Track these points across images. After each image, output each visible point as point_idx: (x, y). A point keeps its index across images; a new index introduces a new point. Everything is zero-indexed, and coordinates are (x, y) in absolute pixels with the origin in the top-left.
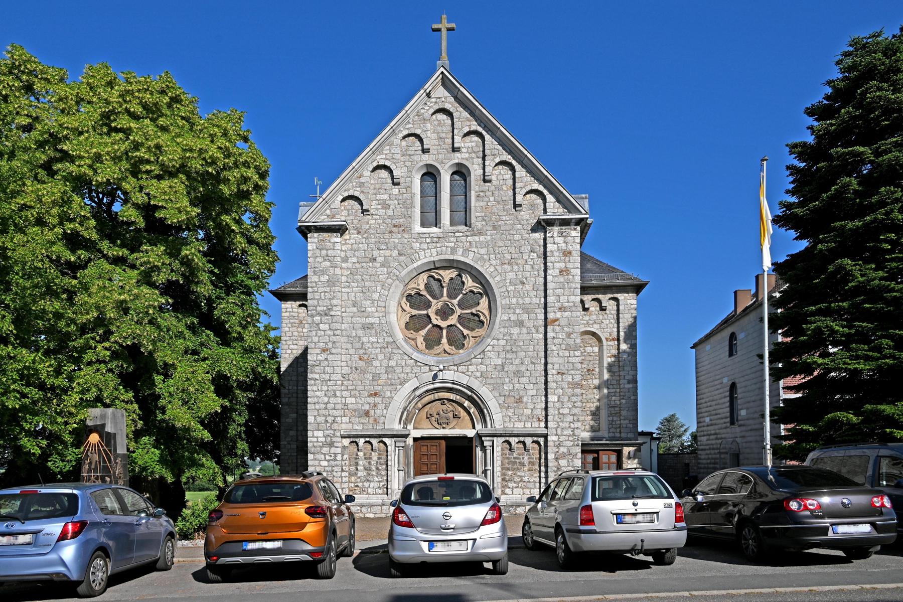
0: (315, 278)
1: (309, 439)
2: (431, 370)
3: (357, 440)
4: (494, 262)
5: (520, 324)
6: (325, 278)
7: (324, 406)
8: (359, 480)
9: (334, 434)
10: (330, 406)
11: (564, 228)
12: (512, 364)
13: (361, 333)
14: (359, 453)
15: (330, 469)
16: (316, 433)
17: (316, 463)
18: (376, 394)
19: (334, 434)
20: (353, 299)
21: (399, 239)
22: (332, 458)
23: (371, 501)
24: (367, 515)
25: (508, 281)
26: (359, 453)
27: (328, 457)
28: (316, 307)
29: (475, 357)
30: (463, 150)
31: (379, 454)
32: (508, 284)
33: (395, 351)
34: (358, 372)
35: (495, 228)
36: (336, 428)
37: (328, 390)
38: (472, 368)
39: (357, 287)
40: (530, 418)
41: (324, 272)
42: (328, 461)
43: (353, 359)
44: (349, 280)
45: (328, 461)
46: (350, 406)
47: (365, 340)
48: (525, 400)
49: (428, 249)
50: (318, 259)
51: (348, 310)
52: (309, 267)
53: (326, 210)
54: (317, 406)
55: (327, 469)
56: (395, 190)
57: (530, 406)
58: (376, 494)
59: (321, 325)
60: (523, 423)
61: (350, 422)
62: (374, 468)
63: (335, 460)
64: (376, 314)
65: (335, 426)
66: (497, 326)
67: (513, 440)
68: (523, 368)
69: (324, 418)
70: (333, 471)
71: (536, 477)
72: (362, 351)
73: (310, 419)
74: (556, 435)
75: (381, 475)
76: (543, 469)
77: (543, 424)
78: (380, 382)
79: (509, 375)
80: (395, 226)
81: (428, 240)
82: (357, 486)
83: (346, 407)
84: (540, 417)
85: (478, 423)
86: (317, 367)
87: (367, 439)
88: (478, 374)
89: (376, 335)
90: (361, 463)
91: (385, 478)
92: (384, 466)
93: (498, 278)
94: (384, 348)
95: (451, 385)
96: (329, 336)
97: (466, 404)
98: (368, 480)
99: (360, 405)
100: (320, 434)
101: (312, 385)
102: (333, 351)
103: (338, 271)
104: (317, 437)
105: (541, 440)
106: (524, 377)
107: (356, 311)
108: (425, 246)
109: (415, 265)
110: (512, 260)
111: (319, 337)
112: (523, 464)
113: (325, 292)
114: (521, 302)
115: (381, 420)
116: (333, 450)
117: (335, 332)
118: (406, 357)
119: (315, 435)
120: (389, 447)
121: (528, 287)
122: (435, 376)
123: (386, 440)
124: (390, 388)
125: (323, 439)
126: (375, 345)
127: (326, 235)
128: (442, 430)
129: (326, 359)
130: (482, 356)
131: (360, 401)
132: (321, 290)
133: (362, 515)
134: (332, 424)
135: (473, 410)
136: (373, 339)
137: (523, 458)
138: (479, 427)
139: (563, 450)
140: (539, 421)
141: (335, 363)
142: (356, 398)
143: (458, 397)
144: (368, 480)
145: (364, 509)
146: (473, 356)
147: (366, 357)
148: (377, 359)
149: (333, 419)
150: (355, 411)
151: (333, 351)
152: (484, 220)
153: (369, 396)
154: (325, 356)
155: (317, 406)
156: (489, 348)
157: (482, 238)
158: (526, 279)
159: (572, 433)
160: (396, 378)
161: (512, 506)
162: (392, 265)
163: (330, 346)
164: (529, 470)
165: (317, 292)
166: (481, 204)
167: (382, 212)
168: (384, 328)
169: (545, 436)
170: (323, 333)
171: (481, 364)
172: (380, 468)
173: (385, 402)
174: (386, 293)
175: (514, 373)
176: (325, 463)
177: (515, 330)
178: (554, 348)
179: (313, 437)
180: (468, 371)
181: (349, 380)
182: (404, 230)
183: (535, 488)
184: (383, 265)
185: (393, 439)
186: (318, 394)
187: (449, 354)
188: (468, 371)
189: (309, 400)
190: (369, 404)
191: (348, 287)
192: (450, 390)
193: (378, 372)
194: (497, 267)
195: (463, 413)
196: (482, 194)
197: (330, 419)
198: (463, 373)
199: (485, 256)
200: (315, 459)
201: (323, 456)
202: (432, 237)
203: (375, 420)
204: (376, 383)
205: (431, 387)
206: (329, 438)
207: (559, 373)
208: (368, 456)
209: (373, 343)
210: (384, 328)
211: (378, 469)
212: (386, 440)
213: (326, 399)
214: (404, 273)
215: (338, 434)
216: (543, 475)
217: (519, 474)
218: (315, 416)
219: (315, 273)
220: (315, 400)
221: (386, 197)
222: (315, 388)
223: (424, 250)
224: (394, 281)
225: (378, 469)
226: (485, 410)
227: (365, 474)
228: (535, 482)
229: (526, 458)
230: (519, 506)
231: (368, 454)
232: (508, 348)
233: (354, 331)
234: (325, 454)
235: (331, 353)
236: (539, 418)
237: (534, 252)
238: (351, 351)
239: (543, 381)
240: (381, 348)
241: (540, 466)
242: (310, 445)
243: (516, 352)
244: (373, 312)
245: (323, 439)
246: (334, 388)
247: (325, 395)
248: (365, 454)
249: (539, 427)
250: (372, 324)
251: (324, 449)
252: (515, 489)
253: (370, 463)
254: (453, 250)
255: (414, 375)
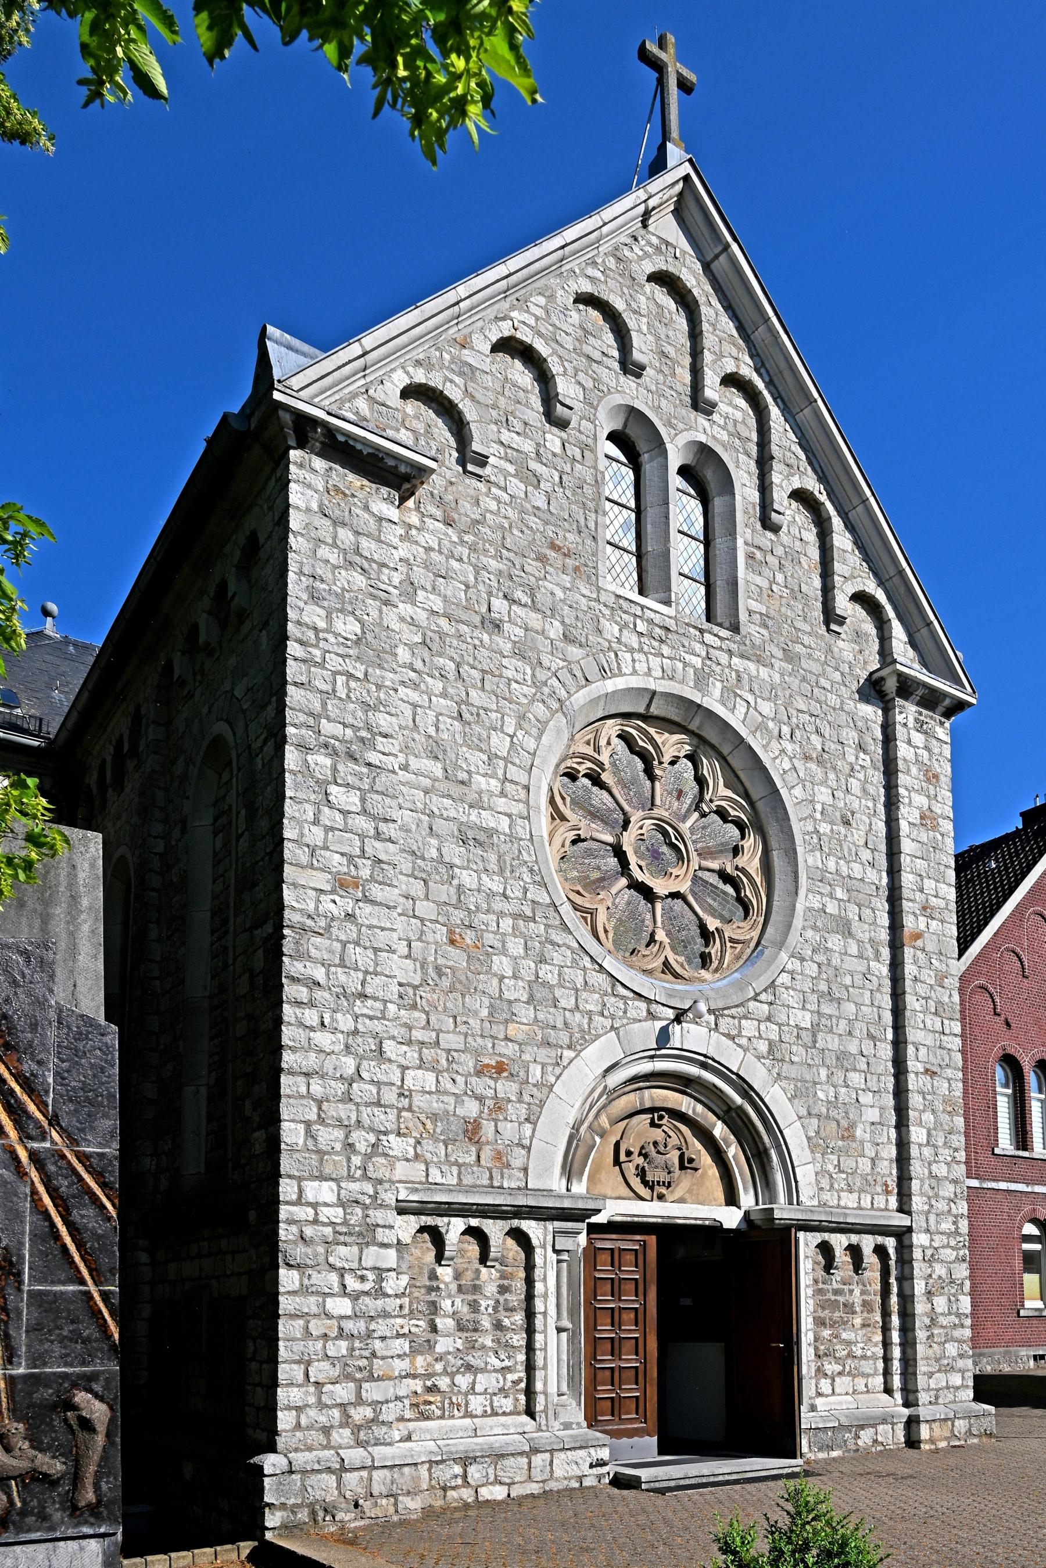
0: (314, 615)
1: (284, 1211)
2: (651, 1016)
3: (440, 1222)
4: (789, 747)
5: (846, 930)
6: (348, 627)
7: (340, 1088)
8: (439, 1367)
9: (374, 1197)
10: (362, 1091)
11: (924, 712)
12: (831, 1031)
13: (454, 852)
14: (440, 1270)
15: (361, 1325)
16: (313, 1190)
17: (311, 1304)
18: (500, 1068)
19: (374, 1197)
20: (432, 731)
21: (565, 589)
22: (367, 1286)
23: (498, 1441)
24: (485, 1493)
25: (819, 807)
26: (440, 1270)
27: (352, 1283)
28: (316, 717)
29: (755, 998)
30: (715, 417)
31: (503, 1276)
32: (818, 816)
33: (558, 937)
34: (445, 983)
35: (789, 657)
36: (383, 1173)
37: (356, 1032)
38: (749, 1027)
39: (444, 695)
40: (868, 1184)
41: (346, 605)
42: (355, 1297)
43: (430, 937)
44: (419, 665)
45: (355, 1297)
46: (418, 1101)
47: (468, 878)
48: (859, 1132)
49: (641, 650)
50: (324, 552)
51: (414, 763)
52: (293, 567)
53: (354, 395)
54: (317, 1088)
55: (349, 1326)
56: (553, 440)
57: (870, 1152)
58: (495, 1414)
59: (333, 789)
60: (856, 1195)
61: (417, 1156)
62: (486, 1323)
63: (379, 1293)
64: (501, 804)
65: (379, 1167)
66: (798, 922)
67: (839, 1242)
68: (853, 1049)
69: (339, 1134)
70: (369, 1334)
71: (876, 1345)
72: (458, 916)
73: (291, 1133)
74: (927, 1231)
75: (507, 1345)
76: (895, 1320)
77: (893, 1202)
78: (512, 1030)
79: (828, 1062)
80: (553, 546)
81: (641, 627)
82: (432, 1389)
83: (405, 1102)
84: (889, 1183)
85: (745, 1189)
86: (318, 940)
87: (474, 1222)
88: (763, 1047)
89: (502, 871)
90: (446, 1304)
91: (521, 1357)
92: (519, 1318)
93: (798, 791)
94: (527, 919)
95: (694, 1070)
96: (362, 837)
97: (719, 1130)
98: (469, 1367)
99: (451, 1100)
100: (323, 1192)
101: (299, 1003)
102: (377, 892)
103: (391, 618)
104: (315, 1206)
105: (890, 1243)
106: (855, 1070)
107: (439, 773)
108: (633, 641)
109: (611, 685)
110: (825, 756)
111: (329, 829)
112: (849, 1308)
113: (350, 676)
114: (844, 870)
115: (517, 1158)
116: (372, 1256)
117: (383, 827)
118: (587, 962)
119: (310, 1195)
120: (538, 1251)
121: (858, 836)
122: (663, 1037)
123: (530, 1227)
124: (543, 1054)
125: (336, 1214)
126: (498, 905)
127: (354, 480)
128: (656, 1204)
129: (350, 916)
130: (771, 998)
131: (449, 1086)
132: (334, 662)
133: (467, 1495)
134: (368, 1157)
135: (733, 1151)
136: (495, 885)
137: (851, 1291)
138: (747, 1200)
139: (940, 1270)
140: (888, 1192)
141: (382, 939)
142: (438, 1073)
143: (700, 1108)
144: (469, 1367)
145: (475, 1473)
146: (752, 994)
147: (469, 937)
148: (504, 952)
149: (372, 1138)
150: (434, 1117)
151: (377, 892)
152: (766, 627)
153: (479, 1073)
154: (349, 905)
155: (317, 1088)
156: (785, 978)
157: (764, 673)
158: (853, 813)
159: (953, 1228)
160: (560, 1024)
161: (848, 1428)
162: (546, 662)
163: (365, 873)
164: (864, 1326)
165: (322, 665)
166: (758, 580)
167: (517, 487)
168: (525, 856)
169: (903, 1235)
170: (339, 817)
171: (769, 1019)
172: (506, 1322)
173: (526, 1098)
174: (531, 744)
175: (838, 1058)
176: (341, 1306)
177: (835, 942)
178: (917, 1006)
179: (299, 1202)
180: (739, 1035)
181: (414, 1007)
182: (576, 569)
183: (875, 1374)
184: (519, 653)
185: (550, 1226)
186: (322, 1039)
187: (677, 976)
188: (739, 1035)
189: (288, 1059)
190: (481, 1099)
191: (416, 686)
192: (683, 1083)
193: (507, 995)
194: (796, 762)
195: (705, 1159)
196: (759, 555)
197: (362, 1140)
198: (728, 1036)
199: (771, 724)
200: (304, 1291)
201: (334, 1278)
202: (651, 622)
203: (498, 1156)
204: (499, 1031)
205: (646, 1067)
206: (358, 1211)
207: (927, 1071)
208: (467, 1279)
209: (491, 895)
210: (525, 856)
211: (498, 1326)
212: (530, 1227)
213: (349, 1065)
214: (580, 697)
215: (390, 1198)
216: (895, 1337)
217: (844, 1336)
218: (308, 1124)
219: (314, 597)
220: (311, 1061)
221: (528, 447)
222: (311, 1017)
223: (632, 650)
224: (553, 713)
225: (498, 1326)
226: (773, 1153)
227: (459, 1344)
228: (874, 1358)
229: (857, 1292)
230: (862, 1427)
231: (469, 1275)
232: (823, 987)
233: (434, 842)
234: (341, 1272)
235: (366, 899)
236: (887, 1186)
237: (865, 752)
238: (425, 909)
239: (891, 1087)
240: (516, 916)
241: (886, 1314)
242: (286, 1233)
243: (839, 1001)
244: (491, 794)
245: (336, 1214)
246: (377, 1026)
247: (347, 1047)
248: (457, 1276)
249: (886, 1209)
250: (490, 832)
251: (342, 1250)
252: (837, 1379)
253: (474, 1306)
254: (701, 680)
255: (608, 1023)
